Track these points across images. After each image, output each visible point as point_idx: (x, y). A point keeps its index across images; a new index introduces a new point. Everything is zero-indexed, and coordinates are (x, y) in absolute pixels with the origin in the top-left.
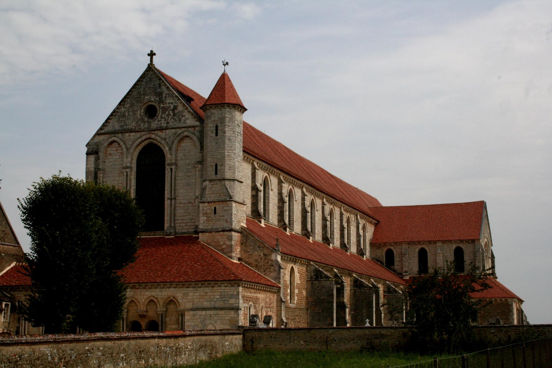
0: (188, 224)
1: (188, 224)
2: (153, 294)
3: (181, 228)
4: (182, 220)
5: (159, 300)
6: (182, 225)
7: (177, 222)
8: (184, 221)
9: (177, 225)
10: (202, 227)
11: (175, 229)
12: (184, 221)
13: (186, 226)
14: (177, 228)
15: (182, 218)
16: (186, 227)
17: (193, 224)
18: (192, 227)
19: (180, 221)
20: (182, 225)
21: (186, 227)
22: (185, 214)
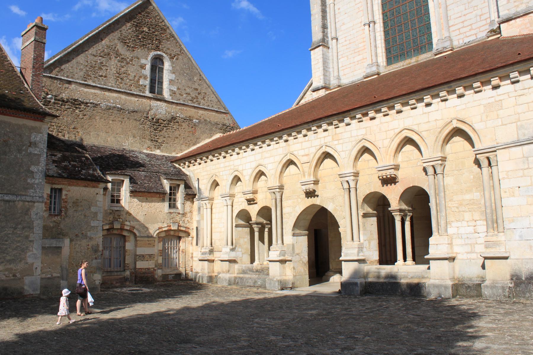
0: (474, 26)
1: (474, 26)
2: (408, 123)
3: (462, 36)
4: (463, 22)
5: (424, 134)
6: (462, 30)
7: (452, 29)
8: (466, 24)
9: (453, 35)
10: (506, 12)
11: (451, 40)
12: (466, 24)
13: (470, 30)
14: (454, 39)
15: (463, 19)
16: (473, 32)
17: (484, 22)
18: (482, 29)
19: (461, 25)
20: (462, 30)
21: (473, 32)
22: (467, 11)
